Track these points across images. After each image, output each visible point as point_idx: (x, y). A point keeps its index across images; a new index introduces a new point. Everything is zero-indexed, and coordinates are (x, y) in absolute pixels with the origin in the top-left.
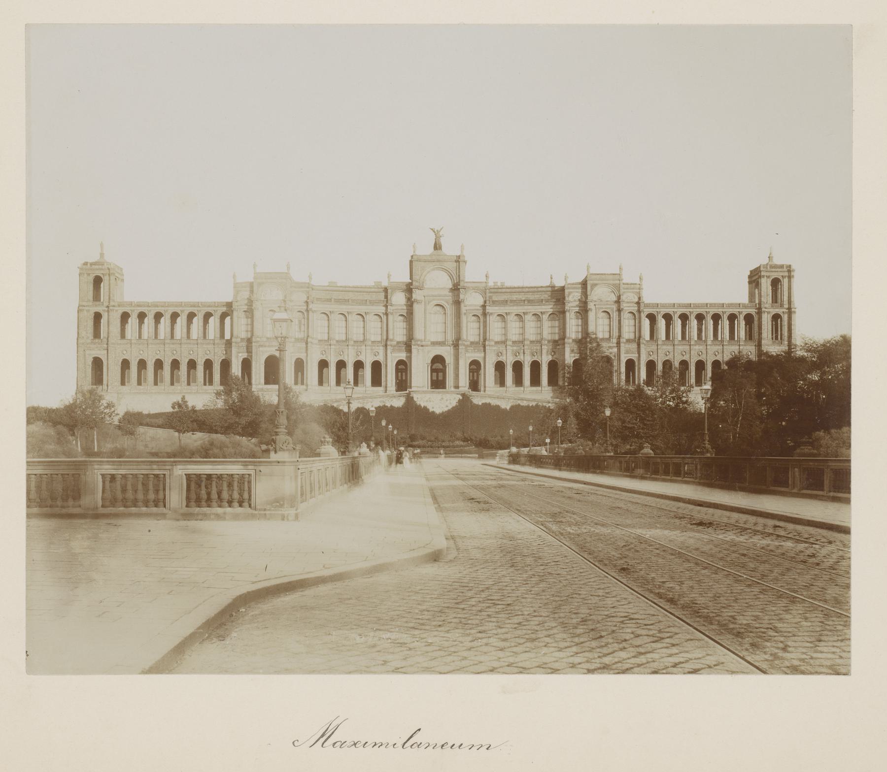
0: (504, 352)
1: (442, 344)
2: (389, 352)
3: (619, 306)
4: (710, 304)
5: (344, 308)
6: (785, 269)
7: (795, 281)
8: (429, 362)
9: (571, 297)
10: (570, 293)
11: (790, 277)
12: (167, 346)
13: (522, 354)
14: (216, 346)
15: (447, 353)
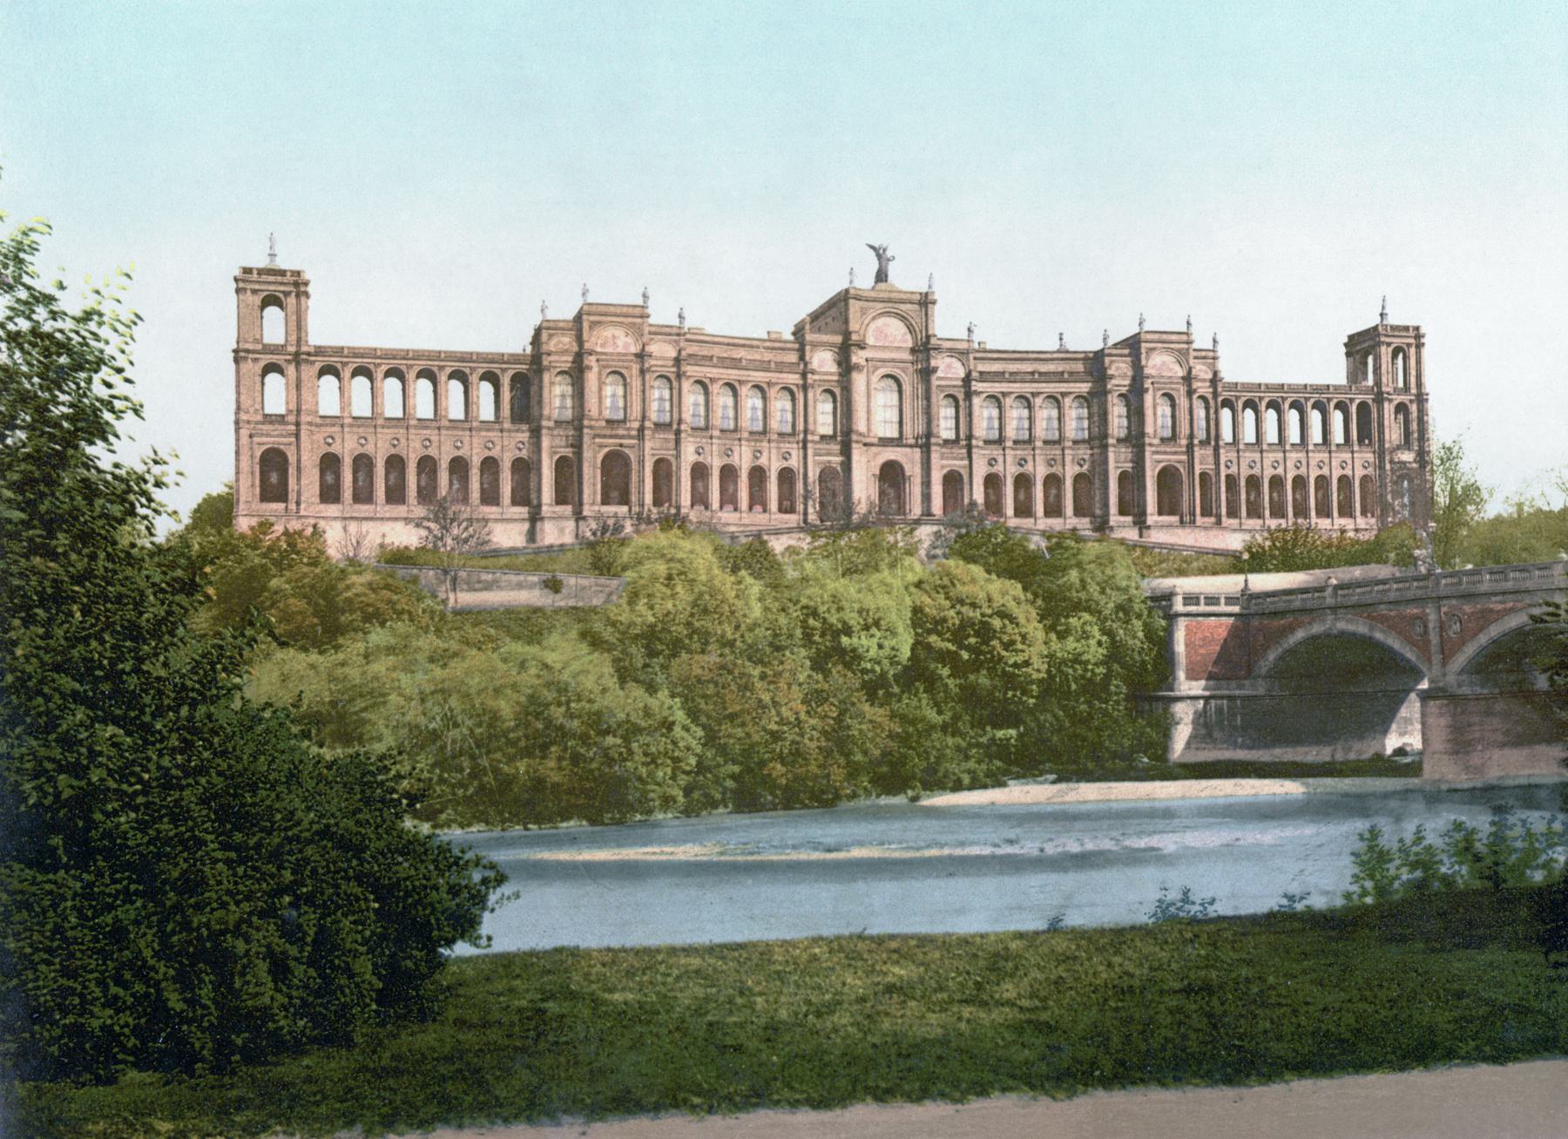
0: (1000, 459)
1: (898, 442)
2: (810, 452)
3: (1190, 385)
4: (1267, 385)
5: (733, 374)
6: (1412, 333)
7: (1426, 352)
8: (878, 472)
9: (1113, 367)
10: (1112, 362)
11: (1419, 346)
12: (412, 431)
13: (1030, 463)
14: (505, 434)
15: (910, 460)
